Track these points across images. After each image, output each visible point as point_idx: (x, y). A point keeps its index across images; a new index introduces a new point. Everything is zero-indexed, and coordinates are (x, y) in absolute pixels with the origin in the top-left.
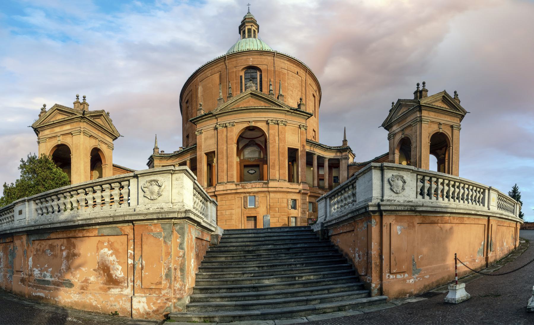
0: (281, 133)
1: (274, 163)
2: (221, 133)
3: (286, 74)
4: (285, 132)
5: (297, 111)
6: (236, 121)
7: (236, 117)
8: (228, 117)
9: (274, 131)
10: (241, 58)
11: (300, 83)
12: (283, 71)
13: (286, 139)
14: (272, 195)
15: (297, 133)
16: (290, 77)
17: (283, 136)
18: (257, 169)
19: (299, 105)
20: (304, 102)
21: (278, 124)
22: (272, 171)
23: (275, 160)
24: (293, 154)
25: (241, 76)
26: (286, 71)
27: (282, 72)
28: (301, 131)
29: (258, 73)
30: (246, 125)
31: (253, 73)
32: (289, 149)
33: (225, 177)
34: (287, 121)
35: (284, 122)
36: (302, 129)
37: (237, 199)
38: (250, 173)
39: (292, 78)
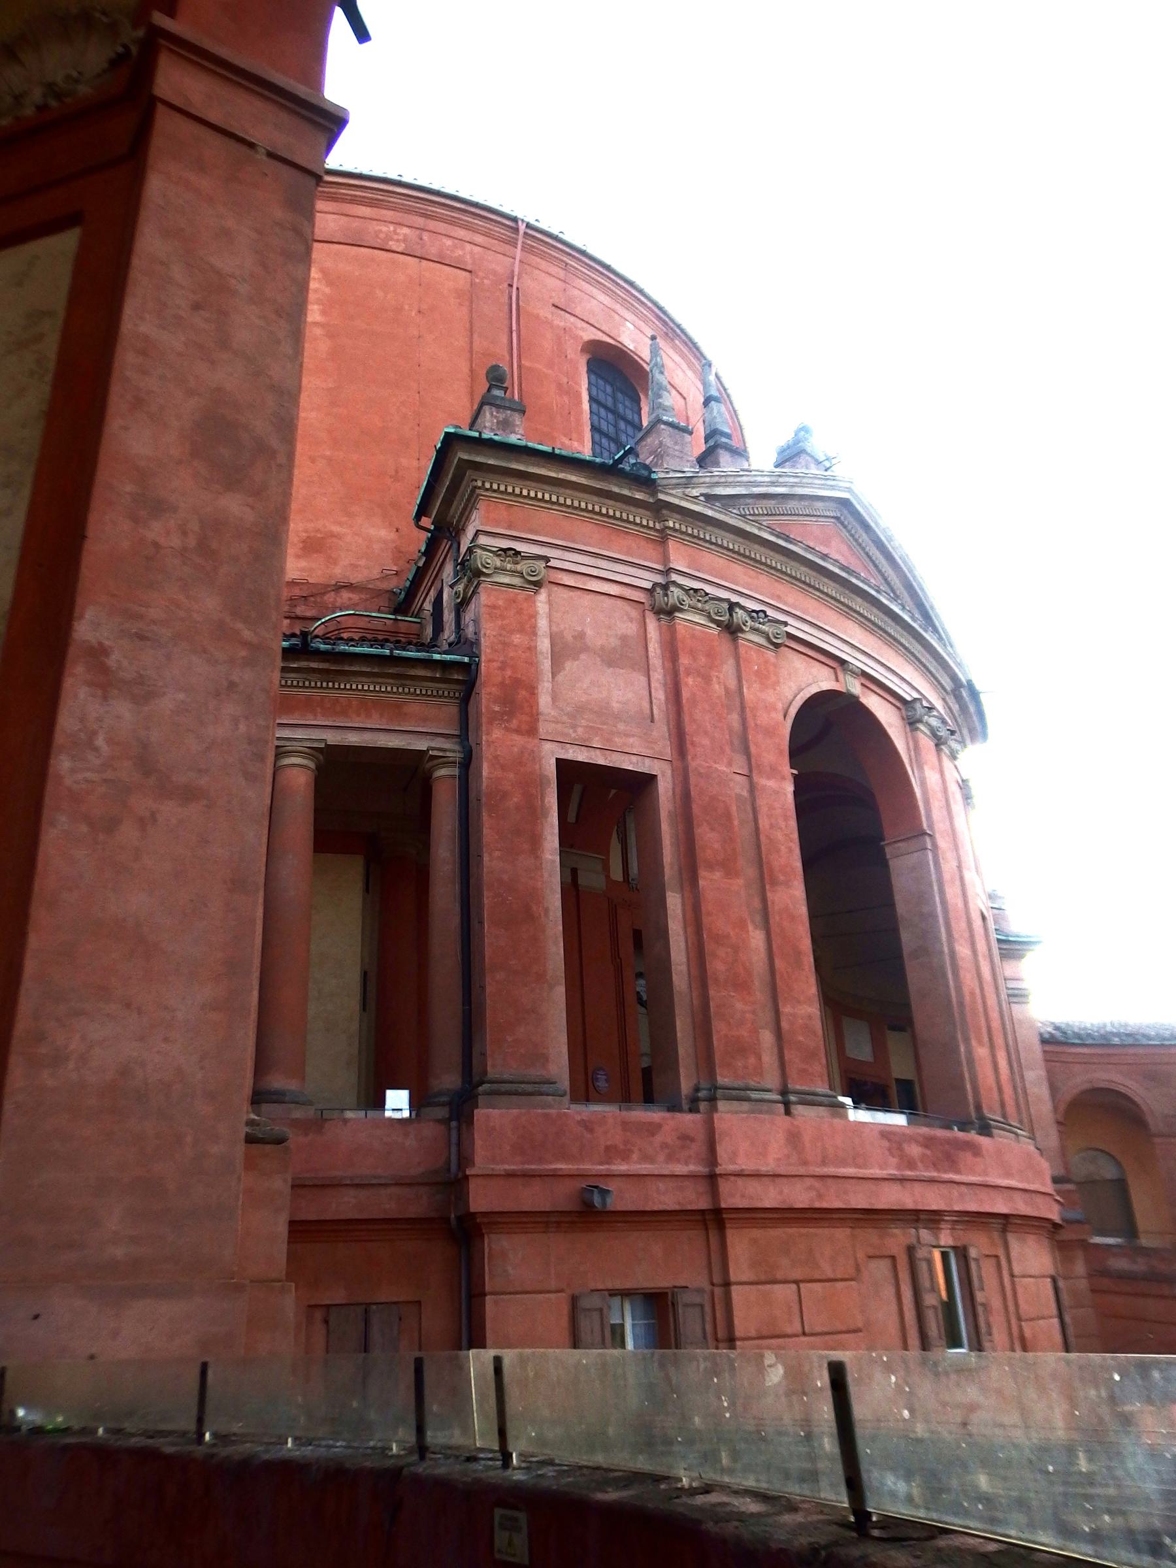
7: (779, 598)
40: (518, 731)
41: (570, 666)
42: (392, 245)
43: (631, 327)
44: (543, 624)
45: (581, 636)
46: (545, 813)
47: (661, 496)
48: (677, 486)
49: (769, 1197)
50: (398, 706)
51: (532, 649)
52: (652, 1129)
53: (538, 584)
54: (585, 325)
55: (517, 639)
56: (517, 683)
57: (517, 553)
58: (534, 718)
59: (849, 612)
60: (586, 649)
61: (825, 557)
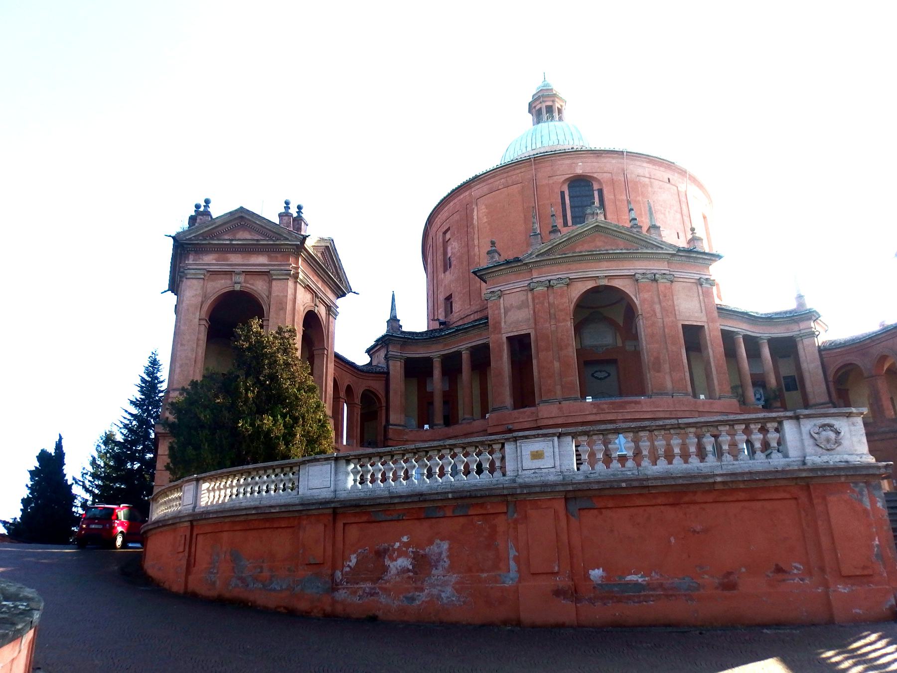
0: (665, 297)
2: (542, 299)
3: (647, 184)
4: (672, 296)
6: (572, 276)
8: (555, 268)
9: (650, 293)
12: (641, 181)
13: (676, 308)
15: (696, 295)
16: (656, 190)
17: (670, 303)
20: (699, 233)
21: (655, 280)
22: (657, 374)
25: (563, 193)
26: (647, 180)
27: (641, 183)
28: (704, 289)
30: (590, 285)
32: (682, 325)
33: (558, 387)
34: (674, 273)
35: (667, 277)
39: (659, 190)
40: (497, 334)
41: (509, 313)
42: (500, 187)
43: (581, 164)
44: (502, 306)
45: (512, 304)
46: (504, 350)
47: (524, 262)
48: (527, 257)
49: (551, 422)
50: (481, 334)
51: (499, 313)
52: (525, 412)
53: (500, 297)
54: (561, 176)
55: (496, 312)
56: (496, 323)
57: (493, 292)
58: (500, 329)
59: (600, 260)
60: (513, 307)
61: (581, 252)
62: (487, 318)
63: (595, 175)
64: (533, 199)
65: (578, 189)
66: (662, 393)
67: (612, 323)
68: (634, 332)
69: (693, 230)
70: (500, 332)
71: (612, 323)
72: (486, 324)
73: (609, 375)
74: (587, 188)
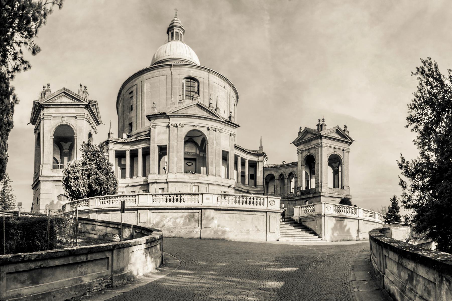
1: (212, 161)
5: (229, 122)
10: (184, 68)
11: (226, 95)
14: (210, 186)
18: (194, 163)
19: (230, 117)
20: (233, 115)
23: (213, 159)
24: (225, 157)
25: (183, 83)
29: (196, 84)
31: (192, 82)
32: (223, 151)
36: (232, 136)
37: (184, 186)
38: (188, 165)
62: (150, 136)
63: (197, 78)
64: (171, 85)
65: (189, 83)
66: (212, 175)
67: (196, 144)
68: (204, 149)
69: (231, 113)
70: (155, 143)
71: (196, 144)
72: (149, 139)
73: (192, 164)
74: (193, 83)
